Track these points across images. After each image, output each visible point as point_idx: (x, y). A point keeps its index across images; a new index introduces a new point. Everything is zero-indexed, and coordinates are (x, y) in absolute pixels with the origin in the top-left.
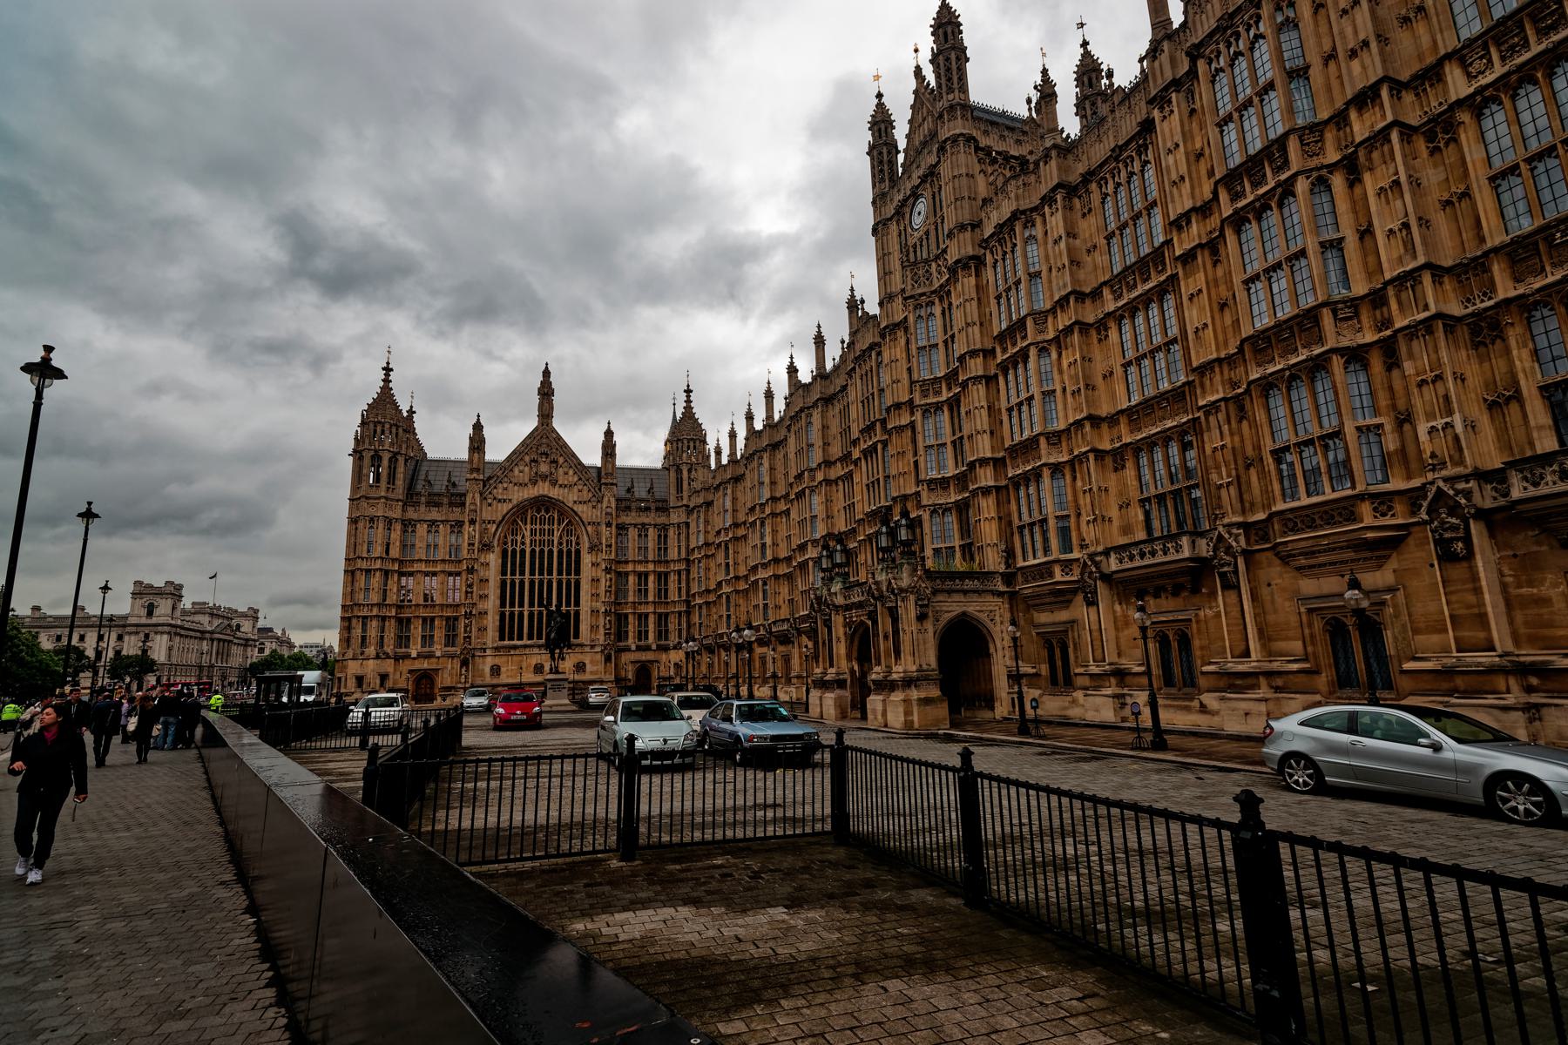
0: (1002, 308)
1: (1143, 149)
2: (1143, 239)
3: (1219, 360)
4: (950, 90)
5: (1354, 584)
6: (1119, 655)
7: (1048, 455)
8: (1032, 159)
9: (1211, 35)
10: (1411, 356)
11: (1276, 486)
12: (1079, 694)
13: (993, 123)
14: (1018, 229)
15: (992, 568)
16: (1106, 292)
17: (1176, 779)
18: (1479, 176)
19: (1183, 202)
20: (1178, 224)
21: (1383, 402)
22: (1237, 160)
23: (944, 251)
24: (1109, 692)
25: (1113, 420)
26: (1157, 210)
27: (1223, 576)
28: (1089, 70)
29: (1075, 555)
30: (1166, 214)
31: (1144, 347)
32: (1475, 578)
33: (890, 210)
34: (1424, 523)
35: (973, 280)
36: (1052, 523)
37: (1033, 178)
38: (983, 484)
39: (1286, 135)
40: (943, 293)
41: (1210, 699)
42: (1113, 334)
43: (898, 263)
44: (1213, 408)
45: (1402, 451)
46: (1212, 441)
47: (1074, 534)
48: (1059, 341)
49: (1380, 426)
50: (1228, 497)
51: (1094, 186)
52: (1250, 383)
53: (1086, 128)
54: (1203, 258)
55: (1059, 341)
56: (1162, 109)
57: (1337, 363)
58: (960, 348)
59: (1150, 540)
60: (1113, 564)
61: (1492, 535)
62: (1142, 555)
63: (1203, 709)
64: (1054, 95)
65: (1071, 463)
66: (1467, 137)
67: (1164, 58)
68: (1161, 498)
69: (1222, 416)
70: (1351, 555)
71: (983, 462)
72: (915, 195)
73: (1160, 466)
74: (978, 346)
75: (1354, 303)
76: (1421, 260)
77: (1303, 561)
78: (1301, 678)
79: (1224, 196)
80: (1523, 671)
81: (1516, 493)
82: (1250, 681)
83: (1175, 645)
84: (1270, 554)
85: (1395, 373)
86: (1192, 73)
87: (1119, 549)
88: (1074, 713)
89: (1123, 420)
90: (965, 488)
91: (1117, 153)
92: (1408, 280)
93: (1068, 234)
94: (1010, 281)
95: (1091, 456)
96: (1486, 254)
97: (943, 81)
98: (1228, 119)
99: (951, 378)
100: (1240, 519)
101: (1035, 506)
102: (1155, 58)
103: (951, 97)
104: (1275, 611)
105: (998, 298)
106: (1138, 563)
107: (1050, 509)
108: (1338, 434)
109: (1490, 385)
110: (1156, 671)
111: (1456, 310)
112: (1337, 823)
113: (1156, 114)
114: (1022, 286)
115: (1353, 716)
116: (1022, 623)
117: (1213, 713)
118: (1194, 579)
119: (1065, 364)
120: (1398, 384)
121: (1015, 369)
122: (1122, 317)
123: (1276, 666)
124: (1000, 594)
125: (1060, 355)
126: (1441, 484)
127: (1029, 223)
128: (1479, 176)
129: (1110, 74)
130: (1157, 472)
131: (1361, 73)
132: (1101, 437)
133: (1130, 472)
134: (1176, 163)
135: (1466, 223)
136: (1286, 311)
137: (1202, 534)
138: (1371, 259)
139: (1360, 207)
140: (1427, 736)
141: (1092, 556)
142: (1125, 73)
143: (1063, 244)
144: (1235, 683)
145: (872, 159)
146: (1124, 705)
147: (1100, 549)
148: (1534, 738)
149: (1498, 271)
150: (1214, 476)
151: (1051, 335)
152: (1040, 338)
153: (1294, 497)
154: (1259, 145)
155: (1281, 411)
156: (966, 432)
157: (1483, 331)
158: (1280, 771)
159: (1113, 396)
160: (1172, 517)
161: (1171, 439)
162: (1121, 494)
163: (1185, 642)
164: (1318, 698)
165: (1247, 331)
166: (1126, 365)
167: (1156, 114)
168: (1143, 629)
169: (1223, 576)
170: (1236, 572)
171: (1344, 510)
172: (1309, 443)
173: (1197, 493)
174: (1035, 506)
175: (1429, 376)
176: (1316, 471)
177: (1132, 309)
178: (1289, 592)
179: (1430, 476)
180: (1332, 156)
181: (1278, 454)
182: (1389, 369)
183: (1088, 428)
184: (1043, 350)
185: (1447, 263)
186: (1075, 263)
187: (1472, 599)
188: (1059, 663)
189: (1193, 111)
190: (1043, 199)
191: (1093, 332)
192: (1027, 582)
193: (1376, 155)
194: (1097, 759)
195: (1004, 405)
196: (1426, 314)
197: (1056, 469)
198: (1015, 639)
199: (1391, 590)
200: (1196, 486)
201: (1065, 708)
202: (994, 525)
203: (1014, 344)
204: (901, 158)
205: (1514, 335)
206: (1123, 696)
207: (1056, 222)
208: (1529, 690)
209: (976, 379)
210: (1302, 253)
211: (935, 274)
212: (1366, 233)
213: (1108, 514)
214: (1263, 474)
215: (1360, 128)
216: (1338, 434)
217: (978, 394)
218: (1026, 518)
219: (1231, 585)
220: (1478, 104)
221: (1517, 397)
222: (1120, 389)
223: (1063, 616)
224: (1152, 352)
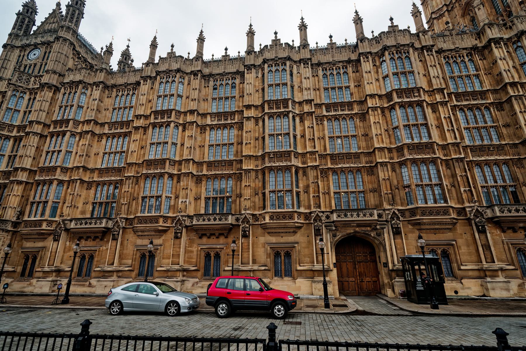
0: (61, 112)
1: (134, 89)
2: (125, 116)
3: (136, 164)
4: (71, 21)
5: (151, 243)
6: (61, 263)
7: (59, 175)
8: (96, 67)
9: (164, 72)
10: (183, 181)
11: (140, 208)
12: (34, 281)
13: (85, 46)
14: (80, 87)
15: (8, 218)
16: (106, 126)
17: (66, 316)
18: (207, 144)
19: (140, 112)
20: (138, 117)
21: (174, 191)
22: (159, 109)
23: (42, 76)
24: (50, 279)
25: (93, 170)
26: (133, 109)
27: (113, 235)
28: (126, 55)
29: (57, 219)
30: (135, 112)
31: (113, 150)
32: (180, 244)
33: (18, 43)
34: (174, 227)
35: (51, 94)
36: (50, 204)
37: (93, 74)
38: (19, 179)
39: (173, 109)
40: (33, 92)
41: (93, 282)
42: (104, 141)
43: (12, 68)
44: (129, 178)
45: (174, 206)
46: (125, 188)
47: (59, 210)
48: (82, 134)
49: (171, 197)
50: (124, 208)
51: (115, 90)
52: (142, 174)
53: (119, 71)
54: (141, 131)
55: (82, 134)
56: (144, 81)
57: (166, 176)
58: (32, 117)
59: (92, 218)
60: (72, 225)
61: (187, 233)
62: (86, 223)
63: (90, 285)
64: (112, 53)
65: (69, 182)
66: (207, 133)
67: (150, 68)
68: (101, 204)
69: (131, 181)
70: (153, 233)
71: (23, 169)
72: (36, 46)
73: (105, 192)
74: (42, 121)
75: (175, 162)
76: (191, 158)
77: (140, 233)
78: (128, 273)
79: (152, 116)
80: (184, 270)
81: (194, 223)
82: (111, 274)
83: (87, 260)
84: (131, 230)
85: (179, 184)
86: (155, 78)
87: (77, 219)
88: (29, 290)
89: (97, 172)
90: (8, 178)
91: (126, 85)
92: (187, 161)
93: (100, 100)
94: (69, 104)
95: (79, 182)
96: (203, 162)
97: (69, 16)
98: (160, 96)
99: (21, 128)
100: (125, 216)
101: (44, 195)
102: (147, 66)
103: (70, 24)
104: (127, 249)
105: (61, 107)
106: (83, 226)
107: (51, 197)
108: (161, 196)
109: (196, 194)
110: (76, 269)
111: (195, 173)
112: (122, 325)
113: (142, 81)
114: (74, 108)
115: (138, 286)
116: (15, 246)
117: (93, 287)
118: (104, 234)
119: (81, 143)
120: (178, 187)
121: (57, 137)
122: (109, 137)
123: (121, 269)
124: (8, 231)
125: (80, 140)
126: (180, 217)
127: (85, 88)
128: (207, 144)
129: (132, 61)
130: (102, 194)
131: (193, 106)
132: (85, 175)
133: (92, 191)
134: (143, 99)
135: (202, 153)
136: (158, 157)
137: (110, 219)
138: (182, 152)
139: (183, 138)
140: (156, 291)
141: (63, 221)
142: (137, 64)
143: (96, 102)
144: (105, 274)
145: (18, 18)
146: (55, 285)
147: (69, 218)
148: (181, 290)
149: (205, 167)
150: (122, 200)
151: (79, 131)
152: (73, 130)
153: (144, 213)
154: (166, 109)
155: (148, 185)
156: (19, 153)
157: (198, 180)
158: (109, 308)
159: (96, 162)
160: (103, 211)
161: (111, 184)
162: (86, 199)
163: (92, 257)
164: (131, 279)
165: (146, 158)
166: (105, 153)
167: (142, 81)
168: (76, 253)
169: (113, 235)
170: (118, 234)
171: (155, 220)
172: (153, 197)
173: (114, 205)
174: (44, 195)
175: (185, 187)
176: (152, 206)
177: (114, 136)
178: (133, 243)
179: (178, 214)
180: (181, 122)
181: (144, 198)
182: (177, 183)
183: (81, 170)
184: (73, 135)
185: (196, 161)
186: (98, 110)
187: (178, 250)
188: (29, 266)
189: (152, 88)
190: (94, 83)
191: (96, 138)
192: (26, 227)
193: (190, 127)
194: (31, 311)
195: (46, 148)
196: (188, 171)
197: (61, 182)
198: (7, 254)
199: (161, 245)
200: (115, 202)
201: (24, 287)
202: (18, 199)
203: (61, 127)
204: (35, 28)
205: (204, 183)
206: (57, 281)
207: (97, 93)
208: (184, 276)
209: (35, 134)
210: (167, 143)
211: (32, 82)
212: (182, 145)
213: (78, 205)
214: (137, 203)
215: (189, 118)
216: (161, 196)
217: (34, 141)
218: (37, 199)
219: (115, 239)
220: (212, 127)
221: (200, 198)
222: (99, 161)
223: (40, 244)
224: (115, 153)
